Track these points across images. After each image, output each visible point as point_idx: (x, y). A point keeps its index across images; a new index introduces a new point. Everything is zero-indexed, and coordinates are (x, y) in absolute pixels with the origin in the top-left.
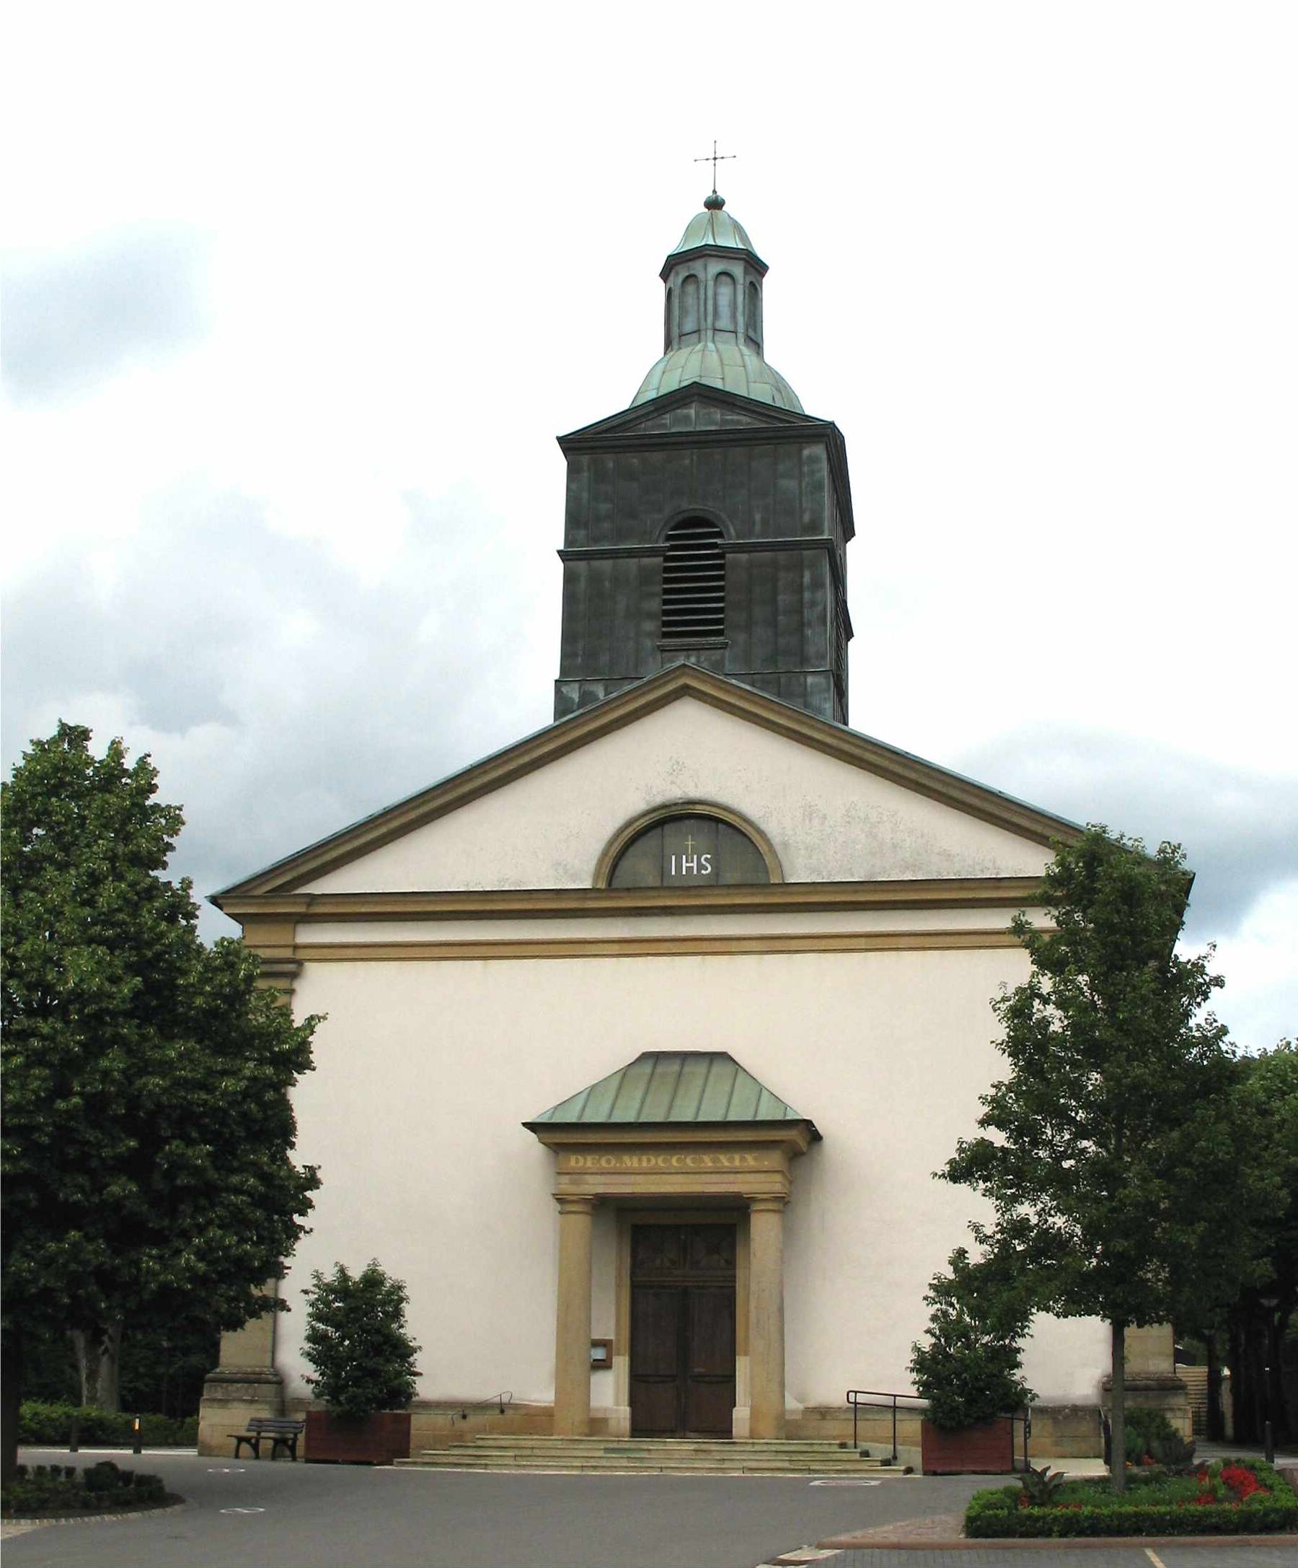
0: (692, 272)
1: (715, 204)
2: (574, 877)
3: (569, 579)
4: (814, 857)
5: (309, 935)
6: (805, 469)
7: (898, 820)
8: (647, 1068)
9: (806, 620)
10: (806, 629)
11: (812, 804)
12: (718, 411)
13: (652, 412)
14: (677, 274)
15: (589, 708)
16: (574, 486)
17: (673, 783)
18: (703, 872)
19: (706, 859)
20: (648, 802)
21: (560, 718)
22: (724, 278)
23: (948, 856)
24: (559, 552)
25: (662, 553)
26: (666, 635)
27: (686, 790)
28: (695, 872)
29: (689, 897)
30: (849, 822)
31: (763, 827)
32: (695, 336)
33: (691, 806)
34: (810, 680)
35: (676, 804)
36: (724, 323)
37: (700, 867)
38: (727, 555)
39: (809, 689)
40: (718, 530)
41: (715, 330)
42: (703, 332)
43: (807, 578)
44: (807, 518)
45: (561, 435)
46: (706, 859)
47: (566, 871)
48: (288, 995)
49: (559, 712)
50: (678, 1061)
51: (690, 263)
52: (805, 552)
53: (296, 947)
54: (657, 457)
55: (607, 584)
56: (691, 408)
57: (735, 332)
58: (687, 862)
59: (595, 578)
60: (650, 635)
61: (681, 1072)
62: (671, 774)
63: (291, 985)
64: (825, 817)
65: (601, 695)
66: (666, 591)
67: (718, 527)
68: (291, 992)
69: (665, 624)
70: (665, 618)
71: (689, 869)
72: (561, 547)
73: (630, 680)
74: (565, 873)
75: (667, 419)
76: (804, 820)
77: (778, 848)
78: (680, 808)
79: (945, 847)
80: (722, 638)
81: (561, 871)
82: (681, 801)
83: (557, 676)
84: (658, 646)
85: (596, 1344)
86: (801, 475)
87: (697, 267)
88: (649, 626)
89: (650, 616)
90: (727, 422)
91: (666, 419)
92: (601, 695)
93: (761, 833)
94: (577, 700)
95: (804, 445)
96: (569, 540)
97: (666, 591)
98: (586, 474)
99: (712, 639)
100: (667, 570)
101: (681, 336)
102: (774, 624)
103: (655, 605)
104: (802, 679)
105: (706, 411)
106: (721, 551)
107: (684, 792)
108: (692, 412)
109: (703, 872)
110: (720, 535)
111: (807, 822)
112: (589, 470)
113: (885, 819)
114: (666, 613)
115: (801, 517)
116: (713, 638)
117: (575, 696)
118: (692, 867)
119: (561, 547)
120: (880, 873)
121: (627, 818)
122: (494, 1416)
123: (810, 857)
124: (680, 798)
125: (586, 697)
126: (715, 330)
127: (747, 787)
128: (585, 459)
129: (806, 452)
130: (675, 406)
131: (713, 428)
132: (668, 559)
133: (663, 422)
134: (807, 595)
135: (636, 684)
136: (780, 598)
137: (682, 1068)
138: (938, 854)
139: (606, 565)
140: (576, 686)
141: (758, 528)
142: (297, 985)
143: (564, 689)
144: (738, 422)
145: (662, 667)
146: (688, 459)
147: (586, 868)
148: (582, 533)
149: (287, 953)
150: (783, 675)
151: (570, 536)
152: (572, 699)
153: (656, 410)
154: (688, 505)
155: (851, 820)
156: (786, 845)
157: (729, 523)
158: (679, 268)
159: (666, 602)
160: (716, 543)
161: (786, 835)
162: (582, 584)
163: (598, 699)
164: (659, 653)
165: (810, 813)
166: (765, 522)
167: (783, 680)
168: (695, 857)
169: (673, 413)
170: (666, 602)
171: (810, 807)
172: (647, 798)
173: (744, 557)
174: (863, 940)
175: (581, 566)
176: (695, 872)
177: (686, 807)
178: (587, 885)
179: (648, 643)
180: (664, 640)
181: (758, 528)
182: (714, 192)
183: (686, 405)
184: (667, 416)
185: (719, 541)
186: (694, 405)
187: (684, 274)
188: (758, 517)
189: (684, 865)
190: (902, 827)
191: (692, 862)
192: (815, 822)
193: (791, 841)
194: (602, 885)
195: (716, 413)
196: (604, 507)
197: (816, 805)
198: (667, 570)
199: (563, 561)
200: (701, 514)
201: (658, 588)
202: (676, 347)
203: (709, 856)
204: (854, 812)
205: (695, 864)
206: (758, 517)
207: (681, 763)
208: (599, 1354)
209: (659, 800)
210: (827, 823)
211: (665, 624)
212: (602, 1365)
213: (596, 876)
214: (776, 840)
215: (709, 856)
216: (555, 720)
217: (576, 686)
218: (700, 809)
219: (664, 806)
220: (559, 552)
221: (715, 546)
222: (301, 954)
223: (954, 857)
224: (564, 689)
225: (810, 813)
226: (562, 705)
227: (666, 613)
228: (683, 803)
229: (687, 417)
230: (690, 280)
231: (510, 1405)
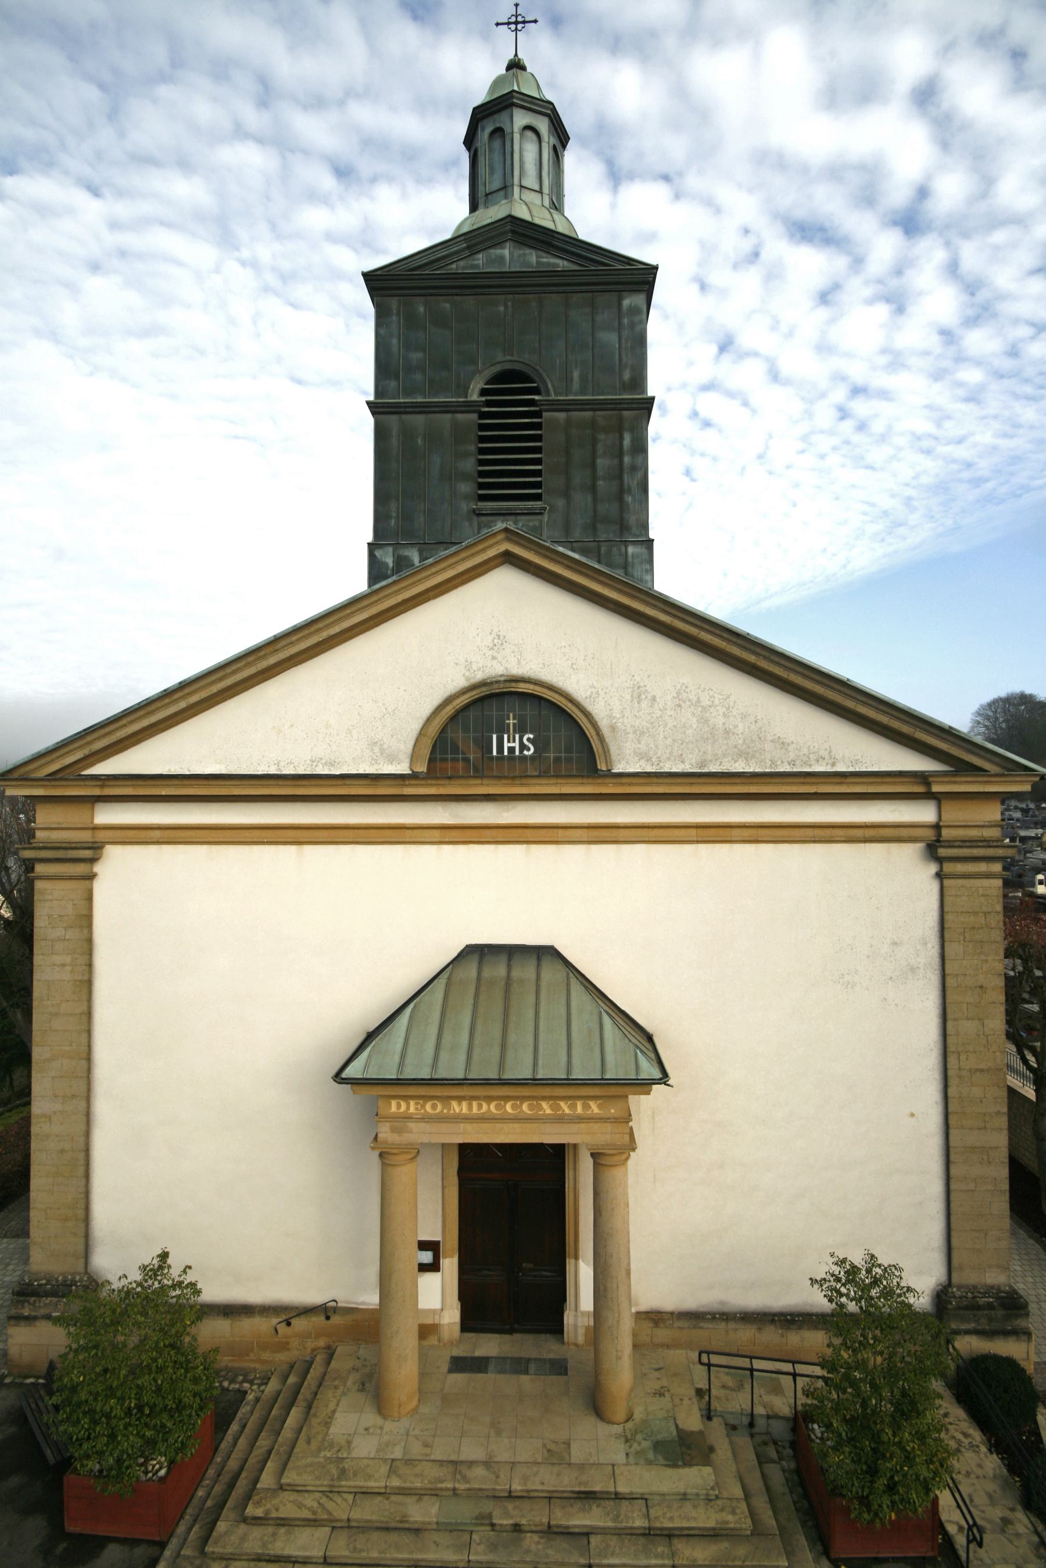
0: (498, 125)
1: (515, 65)
2: (391, 759)
3: (381, 435)
4: (643, 742)
5: (107, 816)
6: (626, 321)
7: (731, 704)
8: (470, 970)
9: (626, 486)
10: (625, 496)
11: (642, 684)
12: (534, 252)
13: (463, 250)
14: (483, 130)
15: (403, 574)
16: (382, 332)
17: (494, 658)
18: (526, 752)
19: (529, 739)
20: (468, 679)
21: (374, 584)
22: (529, 134)
23: (782, 744)
24: (368, 403)
25: (477, 408)
26: (483, 498)
27: (509, 666)
28: (517, 753)
29: (514, 785)
30: (679, 706)
31: (590, 708)
32: (502, 193)
33: (513, 684)
34: (631, 549)
35: (497, 682)
36: (531, 181)
37: (523, 747)
38: (544, 414)
39: (630, 559)
40: (535, 385)
41: (521, 187)
42: (510, 189)
43: (627, 441)
44: (627, 376)
45: (365, 270)
46: (529, 739)
47: (382, 751)
48: (87, 882)
49: (373, 578)
50: (503, 958)
51: (496, 116)
52: (626, 413)
53: (96, 828)
54: (470, 302)
55: (420, 441)
56: (503, 248)
57: (541, 192)
58: (509, 741)
59: (408, 434)
60: (466, 497)
61: (509, 978)
62: (492, 649)
63: (92, 869)
64: (654, 699)
65: (416, 560)
66: (482, 451)
67: (535, 382)
68: (91, 877)
69: (482, 486)
70: (480, 480)
71: (511, 750)
72: (371, 398)
73: (445, 545)
74: (382, 754)
75: (480, 259)
76: (632, 701)
77: (605, 731)
78: (501, 686)
79: (778, 735)
80: (540, 503)
81: (377, 750)
82: (502, 679)
83: (370, 538)
84: (474, 511)
85: (423, 1246)
86: (620, 329)
87: (502, 120)
88: (465, 488)
89: (465, 477)
90: (543, 264)
91: (479, 259)
92: (416, 560)
93: (587, 715)
94: (391, 565)
95: (625, 294)
96: (378, 392)
97: (482, 451)
98: (394, 318)
99: (530, 504)
100: (482, 427)
101: (487, 195)
102: (593, 489)
103: (469, 465)
104: (623, 548)
105: (521, 252)
106: (537, 409)
107: (506, 669)
108: (506, 252)
109: (526, 752)
110: (536, 391)
111: (636, 705)
112: (398, 314)
113: (717, 702)
114: (482, 474)
115: (621, 376)
116: (532, 503)
117: (390, 561)
118: (514, 748)
119: (371, 398)
120: (711, 761)
121: (446, 695)
122: (319, 1320)
123: (639, 742)
124: (501, 676)
125: (401, 563)
126: (521, 187)
127: (572, 664)
128: (394, 303)
129: (626, 303)
130: (487, 244)
131: (530, 270)
132: (483, 415)
133: (476, 262)
134: (627, 459)
135: (454, 549)
136: (599, 461)
137: (509, 972)
138: (772, 741)
139: (419, 420)
140: (390, 549)
141: (576, 384)
142: (97, 868)
143: (378, 553)
144: (555, 265)
145: (479, 533)
146: (502, 306)
147: (402, 747)
148: (393, 384)
149: (86, 836)
150: (603, 543)
151: (380, 387)
152: (387, 564)
153: (468, 248)
154: (502, 361)
155: (681, 703)
156: (613, 728)
157: (548, 380)
158: (485, 122)
159: (482, 463)
160: (534, 399)
161: (614, 718)
162: (394, 442)
163: (413, 565)
164: (475, 518)
165: (638, 694)
166: (583, 378)
167: (603, 549)
168: (517, 736)
169: (485, 252)
170: (482, 463)
171: (639, 687)
172: (467, 674)
173: (561, 416)
174: (693, 832)
175: (393, 420)
176: (517, 753)
177: (507, 685)
178: (402, 768)
179: (465, 506)
180: (480, 504)
181: (576, 384)
182: (516, 55)
183: (500, 244)
184: (480, 256)
185: (536, 397)
186: (508, 244)
187: (489, 129)
188: (576, 374)
189: (506, 745)
190: (735, 712)
191: (514, 741)
192: (644, 704)
193: (619, 724)
194: (422, 768)
195: (531, 254)
196: (416, 356)
197: (645, 686)
198: (482, 427)
199: (373, 414)
200: (517, 367)
201: (472, 448)
202: (481, 206)
203: (531, 736)
204: (685, 695)
205: (517, 745)
206: (576, 374)
207: (502, 637)
208: (427, 1257)
209: (479, 676)
210: (656, 705)
211: (482, 486)
212: (434, 1267)
213: (414, 757)
214: (603, 724)
215: (531, 736)
216: (370, 585)
217: (390, 549)
218: (523, 688)
219: (483, 684)
220: (368, 403)
221: (532, 403)
222: (101, 836)
223: (788, 744)
224: (378, 553)
225: (638, 694)
226: (376, 572)
227: (482, 474)
228: (506, 681)
229: (502, 258)
230: (497, 134)
231: (335, 1310)
